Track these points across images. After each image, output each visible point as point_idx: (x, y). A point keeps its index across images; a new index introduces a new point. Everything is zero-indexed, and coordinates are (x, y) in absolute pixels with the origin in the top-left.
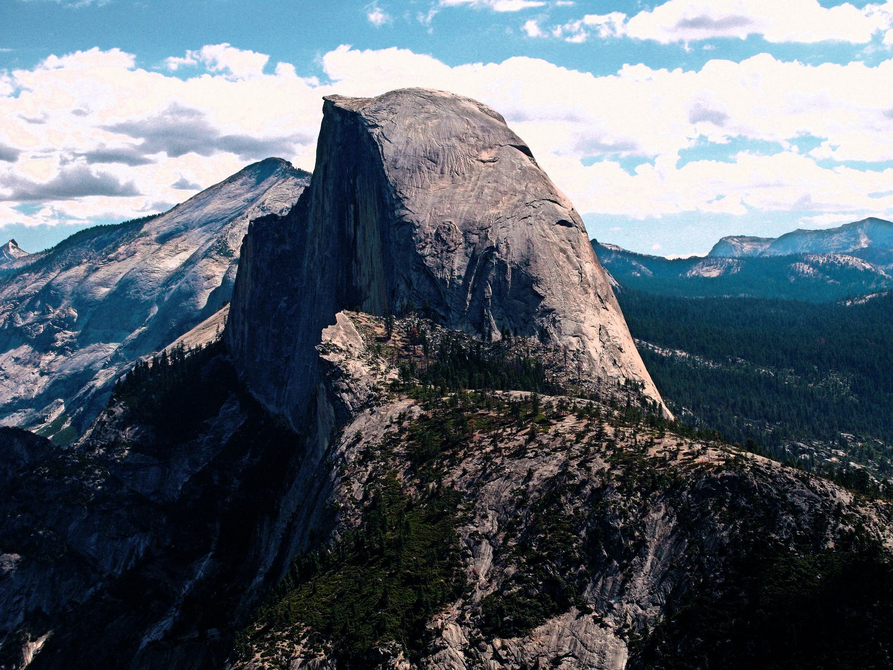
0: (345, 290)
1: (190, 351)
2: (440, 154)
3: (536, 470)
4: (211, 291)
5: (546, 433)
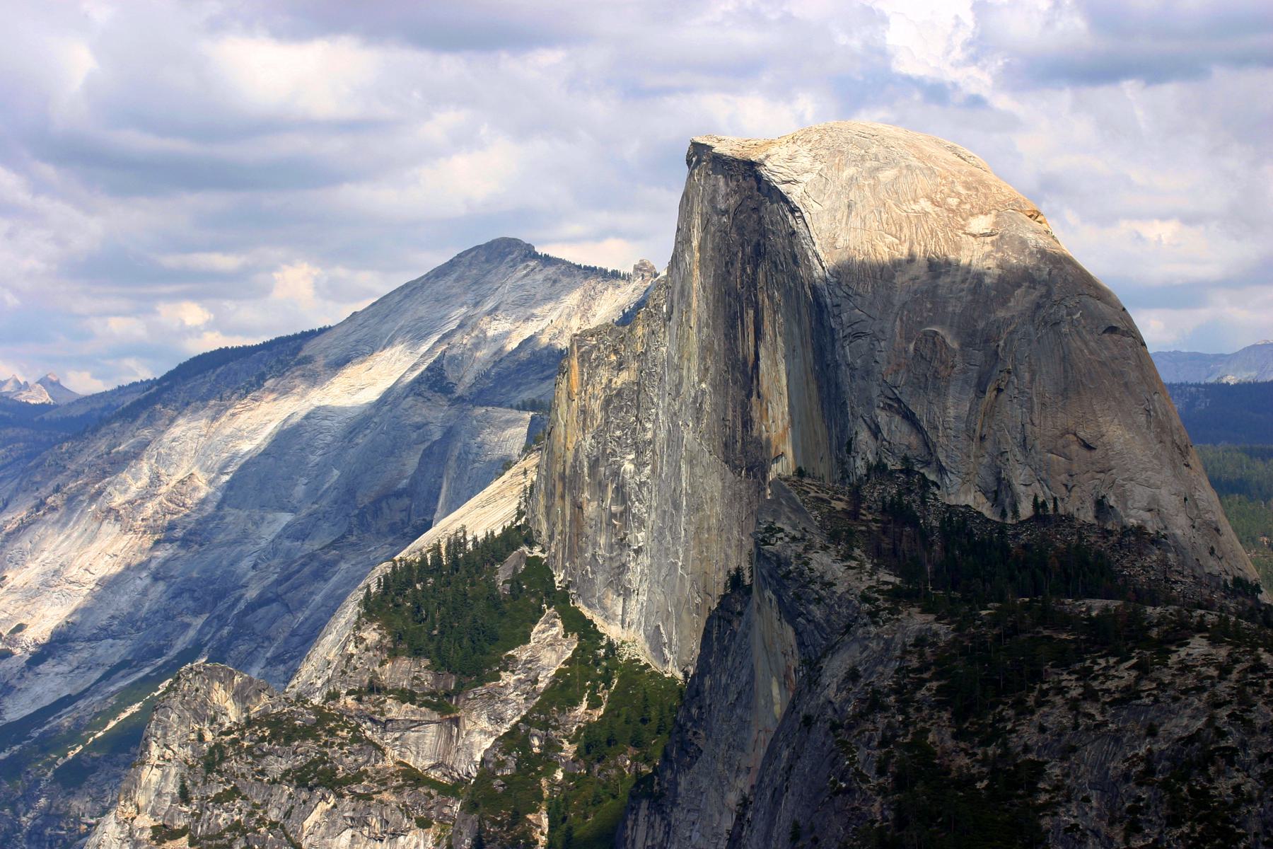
0: (739, 445)
1: (475, 539)
2: (904, 224)
3: (1161, 725)
4: (423, 447)
5: (1166, 666)
